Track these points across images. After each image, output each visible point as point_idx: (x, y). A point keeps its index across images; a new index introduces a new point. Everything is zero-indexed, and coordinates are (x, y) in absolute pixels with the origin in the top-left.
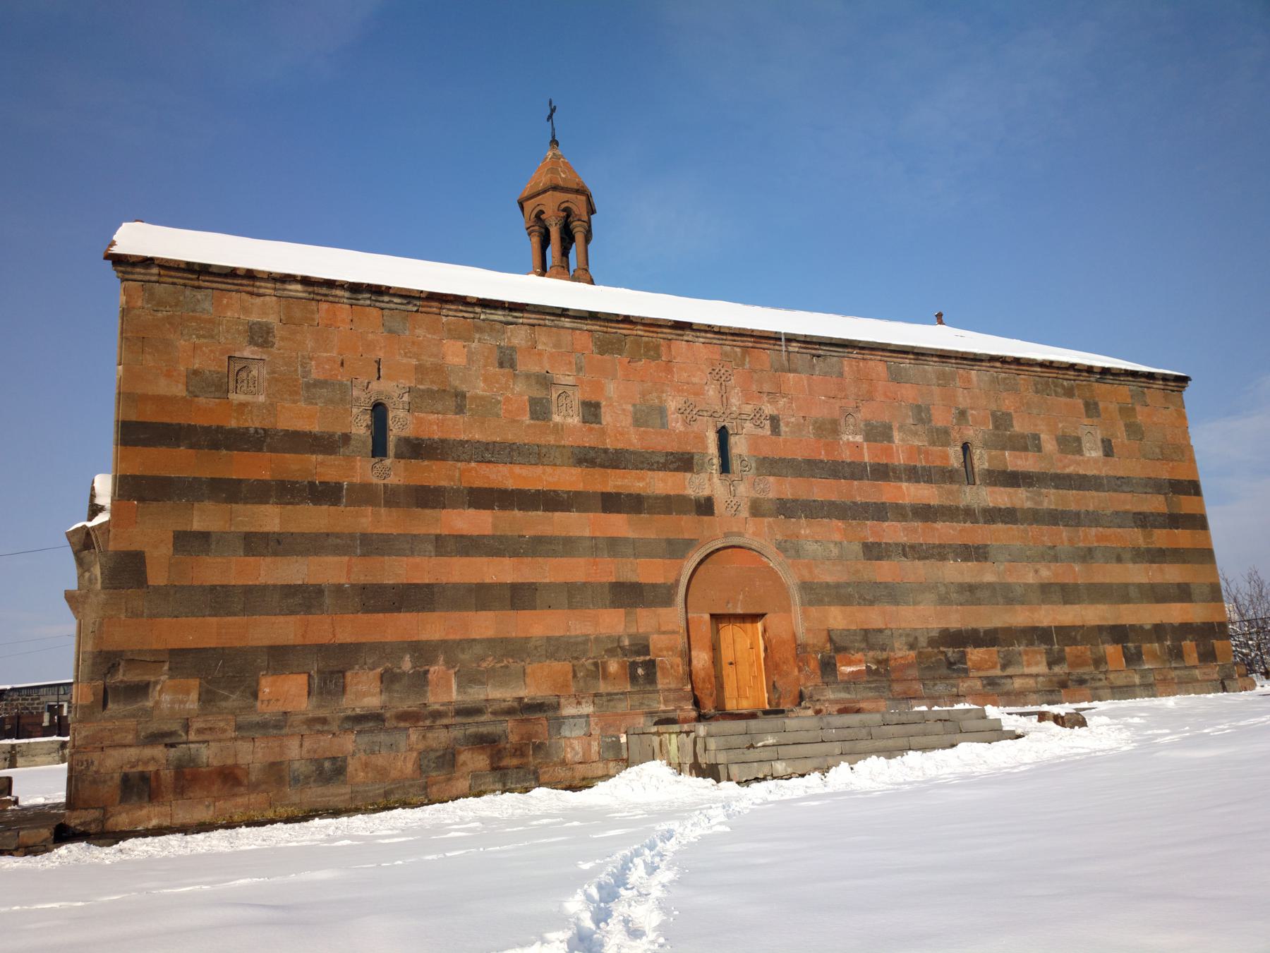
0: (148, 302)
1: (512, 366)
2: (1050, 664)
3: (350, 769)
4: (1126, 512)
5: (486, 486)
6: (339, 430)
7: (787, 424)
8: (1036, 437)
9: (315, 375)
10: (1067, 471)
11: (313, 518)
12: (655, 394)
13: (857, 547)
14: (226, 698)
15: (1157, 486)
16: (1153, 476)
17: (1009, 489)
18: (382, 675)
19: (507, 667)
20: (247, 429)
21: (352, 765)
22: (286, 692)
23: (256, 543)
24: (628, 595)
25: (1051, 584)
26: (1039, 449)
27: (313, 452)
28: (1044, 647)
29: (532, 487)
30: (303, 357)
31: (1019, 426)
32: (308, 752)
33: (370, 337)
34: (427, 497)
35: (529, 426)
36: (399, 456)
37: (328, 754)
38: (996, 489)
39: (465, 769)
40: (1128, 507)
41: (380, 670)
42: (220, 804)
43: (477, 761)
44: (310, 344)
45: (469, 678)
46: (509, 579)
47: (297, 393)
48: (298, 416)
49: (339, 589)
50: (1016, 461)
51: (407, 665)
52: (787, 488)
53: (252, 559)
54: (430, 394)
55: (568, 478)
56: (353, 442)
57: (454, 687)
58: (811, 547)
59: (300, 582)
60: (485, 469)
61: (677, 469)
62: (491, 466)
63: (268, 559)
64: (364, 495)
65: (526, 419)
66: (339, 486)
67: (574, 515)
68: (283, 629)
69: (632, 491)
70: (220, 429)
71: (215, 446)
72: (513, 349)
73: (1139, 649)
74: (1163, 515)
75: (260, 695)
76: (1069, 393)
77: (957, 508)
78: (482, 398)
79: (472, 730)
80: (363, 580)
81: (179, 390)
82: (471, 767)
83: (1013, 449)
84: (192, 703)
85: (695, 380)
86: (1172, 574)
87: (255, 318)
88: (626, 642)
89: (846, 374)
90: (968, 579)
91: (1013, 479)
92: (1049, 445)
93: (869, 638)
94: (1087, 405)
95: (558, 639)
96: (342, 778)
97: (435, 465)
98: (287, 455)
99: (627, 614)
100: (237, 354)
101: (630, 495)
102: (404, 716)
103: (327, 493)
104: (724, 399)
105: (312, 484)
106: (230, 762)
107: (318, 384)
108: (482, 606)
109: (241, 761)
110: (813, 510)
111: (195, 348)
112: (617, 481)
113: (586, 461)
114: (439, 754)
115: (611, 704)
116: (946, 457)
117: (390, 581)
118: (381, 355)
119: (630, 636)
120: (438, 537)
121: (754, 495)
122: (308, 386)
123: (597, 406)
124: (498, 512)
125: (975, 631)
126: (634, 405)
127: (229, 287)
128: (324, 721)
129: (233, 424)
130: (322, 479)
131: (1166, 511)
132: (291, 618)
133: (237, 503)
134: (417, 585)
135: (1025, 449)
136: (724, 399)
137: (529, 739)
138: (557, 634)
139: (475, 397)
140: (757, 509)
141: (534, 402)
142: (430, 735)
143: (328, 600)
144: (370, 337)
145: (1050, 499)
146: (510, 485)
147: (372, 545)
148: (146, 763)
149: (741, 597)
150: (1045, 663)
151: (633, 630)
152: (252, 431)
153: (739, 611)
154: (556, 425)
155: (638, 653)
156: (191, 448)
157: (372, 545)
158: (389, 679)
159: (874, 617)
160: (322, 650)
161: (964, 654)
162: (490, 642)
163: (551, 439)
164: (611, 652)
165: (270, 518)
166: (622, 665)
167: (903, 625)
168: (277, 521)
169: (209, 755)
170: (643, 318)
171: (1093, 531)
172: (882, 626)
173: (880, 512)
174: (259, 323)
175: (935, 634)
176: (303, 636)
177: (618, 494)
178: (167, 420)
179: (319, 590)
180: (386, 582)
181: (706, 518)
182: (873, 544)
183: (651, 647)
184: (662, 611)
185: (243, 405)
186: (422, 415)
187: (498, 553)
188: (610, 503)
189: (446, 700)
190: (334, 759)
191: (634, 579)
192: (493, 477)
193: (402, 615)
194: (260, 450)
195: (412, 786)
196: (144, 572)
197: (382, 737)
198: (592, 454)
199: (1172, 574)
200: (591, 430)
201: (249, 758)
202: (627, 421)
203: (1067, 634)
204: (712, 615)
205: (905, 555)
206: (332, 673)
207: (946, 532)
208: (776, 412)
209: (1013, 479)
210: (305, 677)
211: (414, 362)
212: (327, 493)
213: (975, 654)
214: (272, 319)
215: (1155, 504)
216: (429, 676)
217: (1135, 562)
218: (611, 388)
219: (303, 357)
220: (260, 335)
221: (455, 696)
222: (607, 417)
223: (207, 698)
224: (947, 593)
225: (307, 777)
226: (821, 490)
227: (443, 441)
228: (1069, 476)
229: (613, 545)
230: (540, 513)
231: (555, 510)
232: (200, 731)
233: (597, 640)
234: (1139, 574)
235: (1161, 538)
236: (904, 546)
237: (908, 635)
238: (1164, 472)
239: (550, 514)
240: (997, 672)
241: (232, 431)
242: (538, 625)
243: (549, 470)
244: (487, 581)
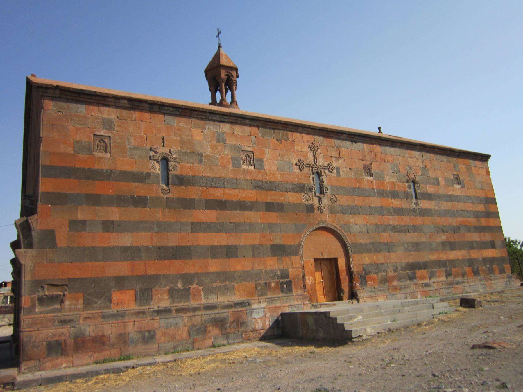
0: (54, 107)
1: (224, 141)
2: (447, 277)
3: (157, 336)
4: (470, 211)
5: (213, 198)
6: (145, 171)
7: (343, 172)
8: (437, 179)
9: (133, 143)
10: (450, 193)
11: (134, 214)
12: (286, 157)
14: (96, 303)
15: (480, 200)
16: (479, 196)
17: (429, 202)
18: (169, 290)
19: (226, 285)
20: (102, 170)
21: (159, 334)
22: (125, 300)
23: (108, 226)
24: (279, 251)
25: (446, 242)
26: (438, 184)
27: (133, 182)
28: (444, 269)
29: (235, 199)
30: (128, 135)
31: (431, 175)
32: (137, 328)
33: (159, 126)
34: (188, 204)
35: (232, 170)
36: (174, 184)
37: (147, 329)
38: (424, 201)
39: (210, 335)
40: (471, 209)
41: (168, 288)
42: (96, 355)
43: (214, 331)
44: (131, 129)
45: (209, 291)
46: (224, 243)
47: (125, 153)
48: (124, 165)
49: (147, 249)
50: (430, 189)
51: (180, 286)
52: (343, 200)
53: (106, 234)
54: (186, 153)
55: (250, 195)
56: (152, 177)
57: (203, 295)
58: (355, 228)
59: (129, 245)
60: (211, 190)
61: (297, 192)
62: (215, 189)
63: (114, 234)
64: (156, 202)
65: (231, 167)
66: (145, 198)
67: (253, 213)
68: (121, 268)
69: (280, 202)
70: (89, 169)
71: (88, 178)
72: (224, 133)
73: (478, 268)
74: (482, 212)
75: (113, 301)
77: (410, 209)
78: (210, 156)
79: (212, 316)
80: (158, 244)
81: (70, 150)
82: (212, 334)
83: (430, 184)
84: (80, 305)
85: (304, 150)
86: (487, 237)
87: (105, 116)
88: (279, 273)
89: (365, 150)
91: (429, 197)
92: (442, 182)
93: (378, 267)
94: (454, 165)
95: (248, 272)
96: (154, 340)
97: (190, 188)
98: (121, 183)
99: (278, 260)
100: (97, 133)
101: (278, 203)
102: (179, 310)
103: (140, 202)
105: (133, 197)
106: (100, 334)
107: (135, 148)
108: (214, 256)
109: (105, 334)
110: (354, 210)
111: (78, 130)
112: (271, 197)
113: (258, 187)
114: (198, 327)
115: (274, 302)
116: (405, 187)
117: (171, 245)
118: (163, 134)
119: (280, 270)
120: (192, 223)
121: (330, 203)
122: (130, 149)
123: (261, 161)
124: (219, 212)
125: (419, 263)
126: (278, 161)
127: (93, 101)
128: (143, 313)
129: (96, 167)
130: (138, 195)
131: (483, 210)
132: (126, 263)
133: (98, 206)
134: (183, 247)
135: (434, 184)
136: (315, 160)
137: (238, 320)
138: (248, 270)
139: (207, 156)
141: (233, 159)
142: (193, 319)
143: (142, 254)
144: (159, 126)
145: (446, 205)
146: (223, 198)
147: (162, 227)
148: (60, 335)
149: (326, 251)
150: (444, 276)
151: (281, 267)
152: (105, 171)
153: (326, 257)
154: (244, 170)
155: (284, 278)
156: (76, 179)
157: (162, 227)
158: (172, 293)
159: (380, 258)
160: (140, 278)
161: (415, 273)
162: (218, 274)
163: (242, 177)
164: (273, 278)
165: (114, 214)
166: (277, 284)
167: (392, 261)
168: (117, 215)
169: (90, 330)
170: (281, 121)
171: (460, 219)
172: (383, 262)
173: (381, 211)
174: (107, 119)
175: (404, 265)
176: (132, 272)
177: (273, 203)
178: (64, 165)
179: (138, 249)
180: (169, 245)
181: (311, 214)
182: (379, 225)
183: (290, 275)
184: (294, 258)
185: (100, 158)
186: (183, 164)
187: (219, 231)
188: (270, 207)
189: (199, 303)
190: (149, 331)
191: (281, 242)
192: (216, 194)
193: (177, 261)
194: (109, 180)
195: (186, 343)
196: (55, 240)
197: (172, 320)
198: (260, 184)
199: (487, 237)
200: (259, 172)
201: (109, 332)
202: (274, 168)
203: (452, 263)
204: (315, 260)
205: (392, 230)
206: (146, 289)
207: (407, 220)
208: (338, 166)
209: (429, 197)
210: (134, 291)
211: (179, 139)
212: (140, 202)
213: (419, 273)
214: (113, 117)
215: (481, 208)
216: (191, 291)
217: (475, 232)
218: (267, 153)
219: (128, 135)
220: (108, 124)
221: (204, 301)
222: (266, 167)
223: (88, 304)
224: (408, 247)
225: (138, 341)
226: (357, 201)
227: (193, 176)
228: (450, 196)
229: (271, 226)
230: (238, 212)
231: (245, 210)
232: (86, 318)
233: (266, 272)
234: (476, 237)
235: (483, 222)
236: (391, 225)
237: (394, 266)
238: (482, 194)
239: (242, 212)
240: (427, 281)
241: (96, 171)
242: (238, 266)
243: (241, 191)
244: (215, 244)
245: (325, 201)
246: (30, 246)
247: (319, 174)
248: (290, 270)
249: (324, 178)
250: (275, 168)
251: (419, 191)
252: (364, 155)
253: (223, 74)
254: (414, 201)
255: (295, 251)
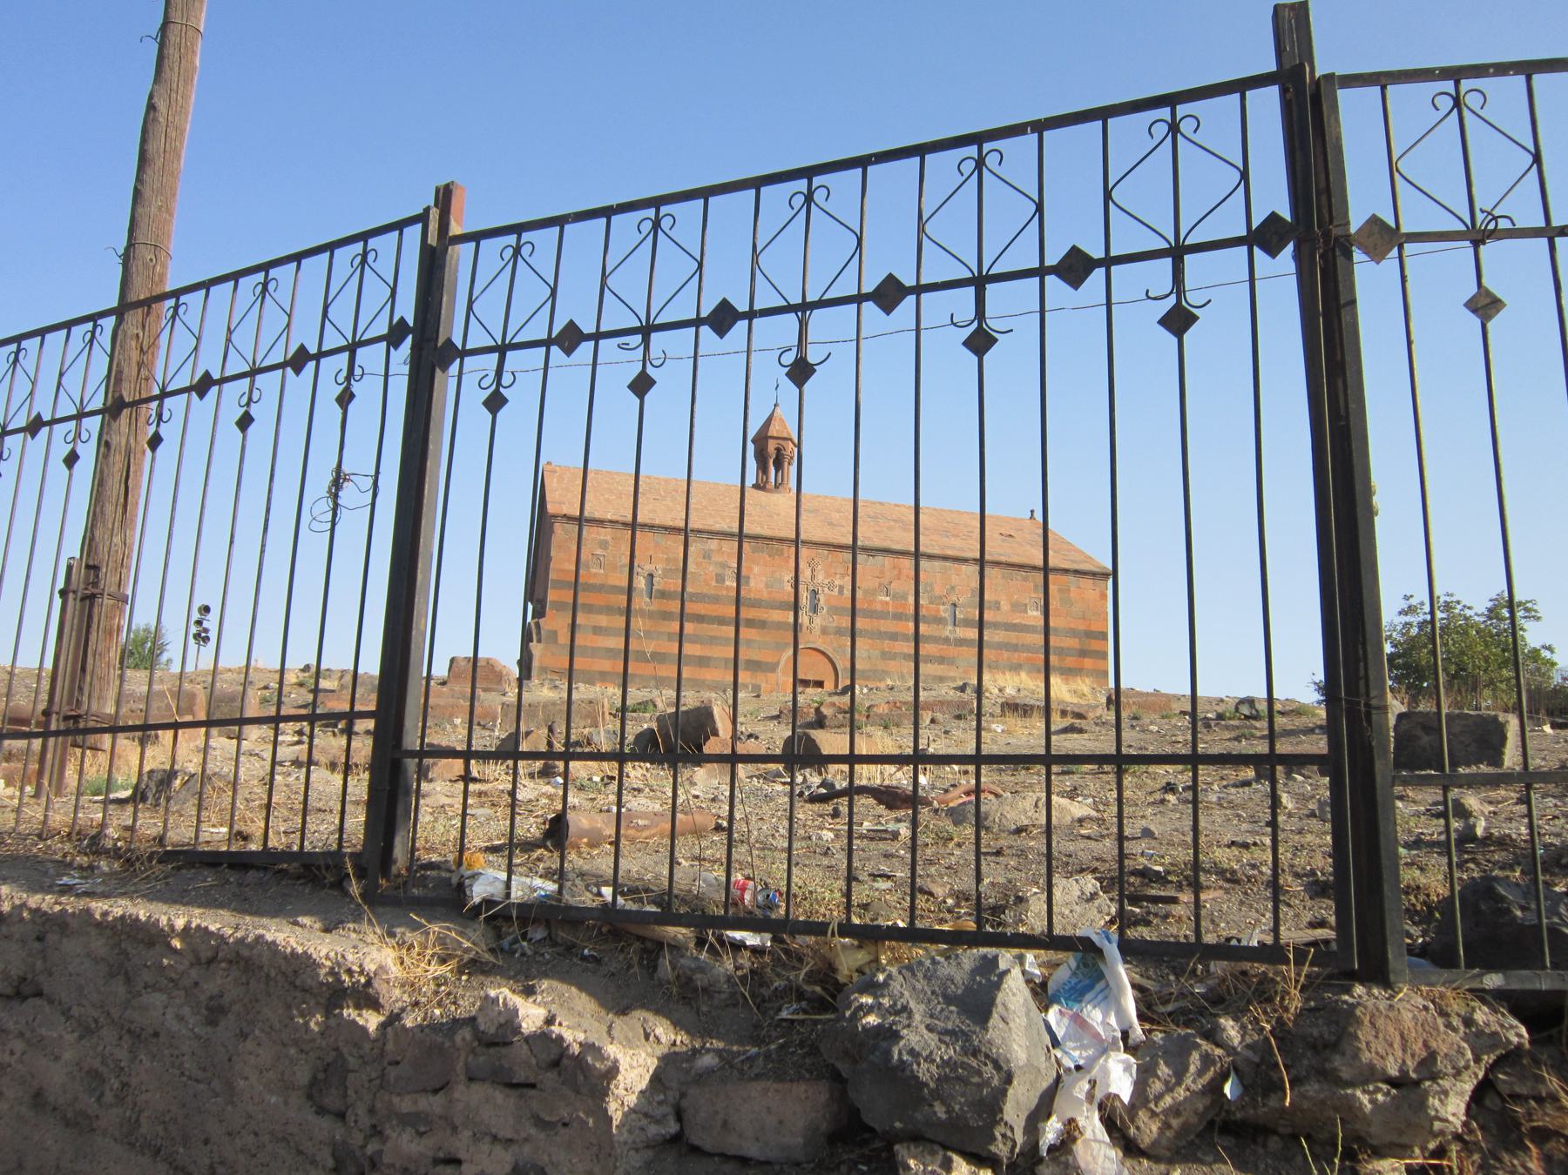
8: (997, 603)
13: (877, 653)
76: (1025, 579)
90: (939, 673)
92: (1005, 606)
104: (813, 577)
136: (813, 577)
140: (824, 631)
191: (756, 658)
238: (1081, 627)
245: (818, 621)
246: (539, 641)
247: (815, 593)
248: (763, 685)
249: (821, 597)
250: (762, 586)
251: (959, 616)
252: (882, 572)
253: (772, 446)
254: (950, 628)
255: (772, 668)
